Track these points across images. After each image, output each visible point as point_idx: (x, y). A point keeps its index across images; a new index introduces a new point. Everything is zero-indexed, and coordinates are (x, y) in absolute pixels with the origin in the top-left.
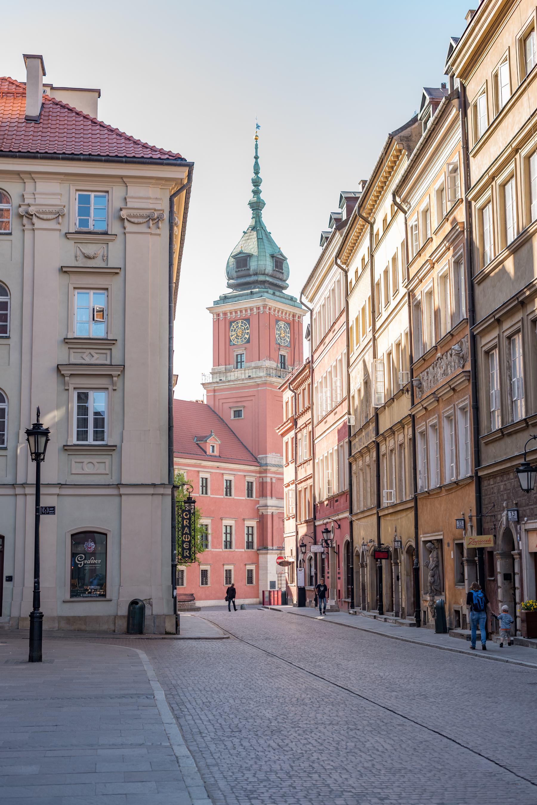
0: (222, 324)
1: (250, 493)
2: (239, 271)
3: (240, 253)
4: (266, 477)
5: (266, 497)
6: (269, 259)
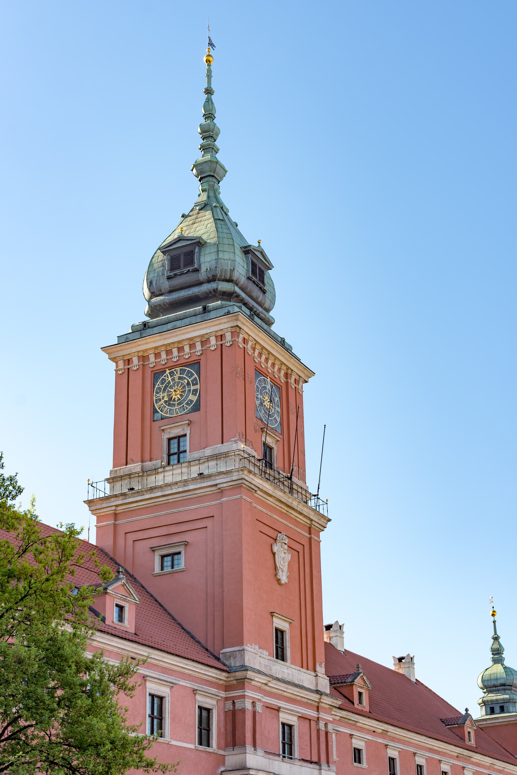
0: (136, 380)
1: (204, 738)
2: (176, 275)
3: (180, 239)
4: (244, 697)
5: (243, 745)
6: (239, 253)
